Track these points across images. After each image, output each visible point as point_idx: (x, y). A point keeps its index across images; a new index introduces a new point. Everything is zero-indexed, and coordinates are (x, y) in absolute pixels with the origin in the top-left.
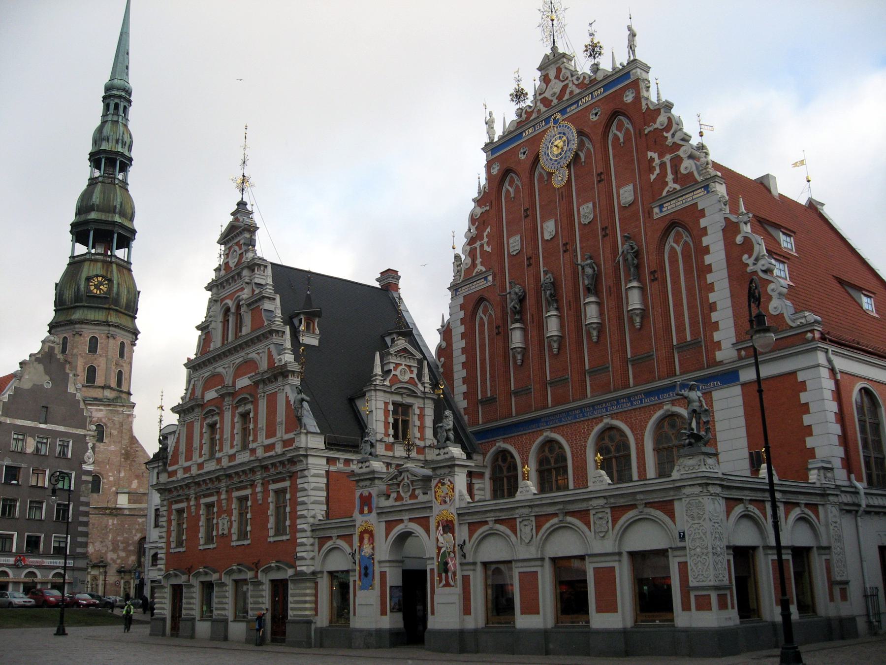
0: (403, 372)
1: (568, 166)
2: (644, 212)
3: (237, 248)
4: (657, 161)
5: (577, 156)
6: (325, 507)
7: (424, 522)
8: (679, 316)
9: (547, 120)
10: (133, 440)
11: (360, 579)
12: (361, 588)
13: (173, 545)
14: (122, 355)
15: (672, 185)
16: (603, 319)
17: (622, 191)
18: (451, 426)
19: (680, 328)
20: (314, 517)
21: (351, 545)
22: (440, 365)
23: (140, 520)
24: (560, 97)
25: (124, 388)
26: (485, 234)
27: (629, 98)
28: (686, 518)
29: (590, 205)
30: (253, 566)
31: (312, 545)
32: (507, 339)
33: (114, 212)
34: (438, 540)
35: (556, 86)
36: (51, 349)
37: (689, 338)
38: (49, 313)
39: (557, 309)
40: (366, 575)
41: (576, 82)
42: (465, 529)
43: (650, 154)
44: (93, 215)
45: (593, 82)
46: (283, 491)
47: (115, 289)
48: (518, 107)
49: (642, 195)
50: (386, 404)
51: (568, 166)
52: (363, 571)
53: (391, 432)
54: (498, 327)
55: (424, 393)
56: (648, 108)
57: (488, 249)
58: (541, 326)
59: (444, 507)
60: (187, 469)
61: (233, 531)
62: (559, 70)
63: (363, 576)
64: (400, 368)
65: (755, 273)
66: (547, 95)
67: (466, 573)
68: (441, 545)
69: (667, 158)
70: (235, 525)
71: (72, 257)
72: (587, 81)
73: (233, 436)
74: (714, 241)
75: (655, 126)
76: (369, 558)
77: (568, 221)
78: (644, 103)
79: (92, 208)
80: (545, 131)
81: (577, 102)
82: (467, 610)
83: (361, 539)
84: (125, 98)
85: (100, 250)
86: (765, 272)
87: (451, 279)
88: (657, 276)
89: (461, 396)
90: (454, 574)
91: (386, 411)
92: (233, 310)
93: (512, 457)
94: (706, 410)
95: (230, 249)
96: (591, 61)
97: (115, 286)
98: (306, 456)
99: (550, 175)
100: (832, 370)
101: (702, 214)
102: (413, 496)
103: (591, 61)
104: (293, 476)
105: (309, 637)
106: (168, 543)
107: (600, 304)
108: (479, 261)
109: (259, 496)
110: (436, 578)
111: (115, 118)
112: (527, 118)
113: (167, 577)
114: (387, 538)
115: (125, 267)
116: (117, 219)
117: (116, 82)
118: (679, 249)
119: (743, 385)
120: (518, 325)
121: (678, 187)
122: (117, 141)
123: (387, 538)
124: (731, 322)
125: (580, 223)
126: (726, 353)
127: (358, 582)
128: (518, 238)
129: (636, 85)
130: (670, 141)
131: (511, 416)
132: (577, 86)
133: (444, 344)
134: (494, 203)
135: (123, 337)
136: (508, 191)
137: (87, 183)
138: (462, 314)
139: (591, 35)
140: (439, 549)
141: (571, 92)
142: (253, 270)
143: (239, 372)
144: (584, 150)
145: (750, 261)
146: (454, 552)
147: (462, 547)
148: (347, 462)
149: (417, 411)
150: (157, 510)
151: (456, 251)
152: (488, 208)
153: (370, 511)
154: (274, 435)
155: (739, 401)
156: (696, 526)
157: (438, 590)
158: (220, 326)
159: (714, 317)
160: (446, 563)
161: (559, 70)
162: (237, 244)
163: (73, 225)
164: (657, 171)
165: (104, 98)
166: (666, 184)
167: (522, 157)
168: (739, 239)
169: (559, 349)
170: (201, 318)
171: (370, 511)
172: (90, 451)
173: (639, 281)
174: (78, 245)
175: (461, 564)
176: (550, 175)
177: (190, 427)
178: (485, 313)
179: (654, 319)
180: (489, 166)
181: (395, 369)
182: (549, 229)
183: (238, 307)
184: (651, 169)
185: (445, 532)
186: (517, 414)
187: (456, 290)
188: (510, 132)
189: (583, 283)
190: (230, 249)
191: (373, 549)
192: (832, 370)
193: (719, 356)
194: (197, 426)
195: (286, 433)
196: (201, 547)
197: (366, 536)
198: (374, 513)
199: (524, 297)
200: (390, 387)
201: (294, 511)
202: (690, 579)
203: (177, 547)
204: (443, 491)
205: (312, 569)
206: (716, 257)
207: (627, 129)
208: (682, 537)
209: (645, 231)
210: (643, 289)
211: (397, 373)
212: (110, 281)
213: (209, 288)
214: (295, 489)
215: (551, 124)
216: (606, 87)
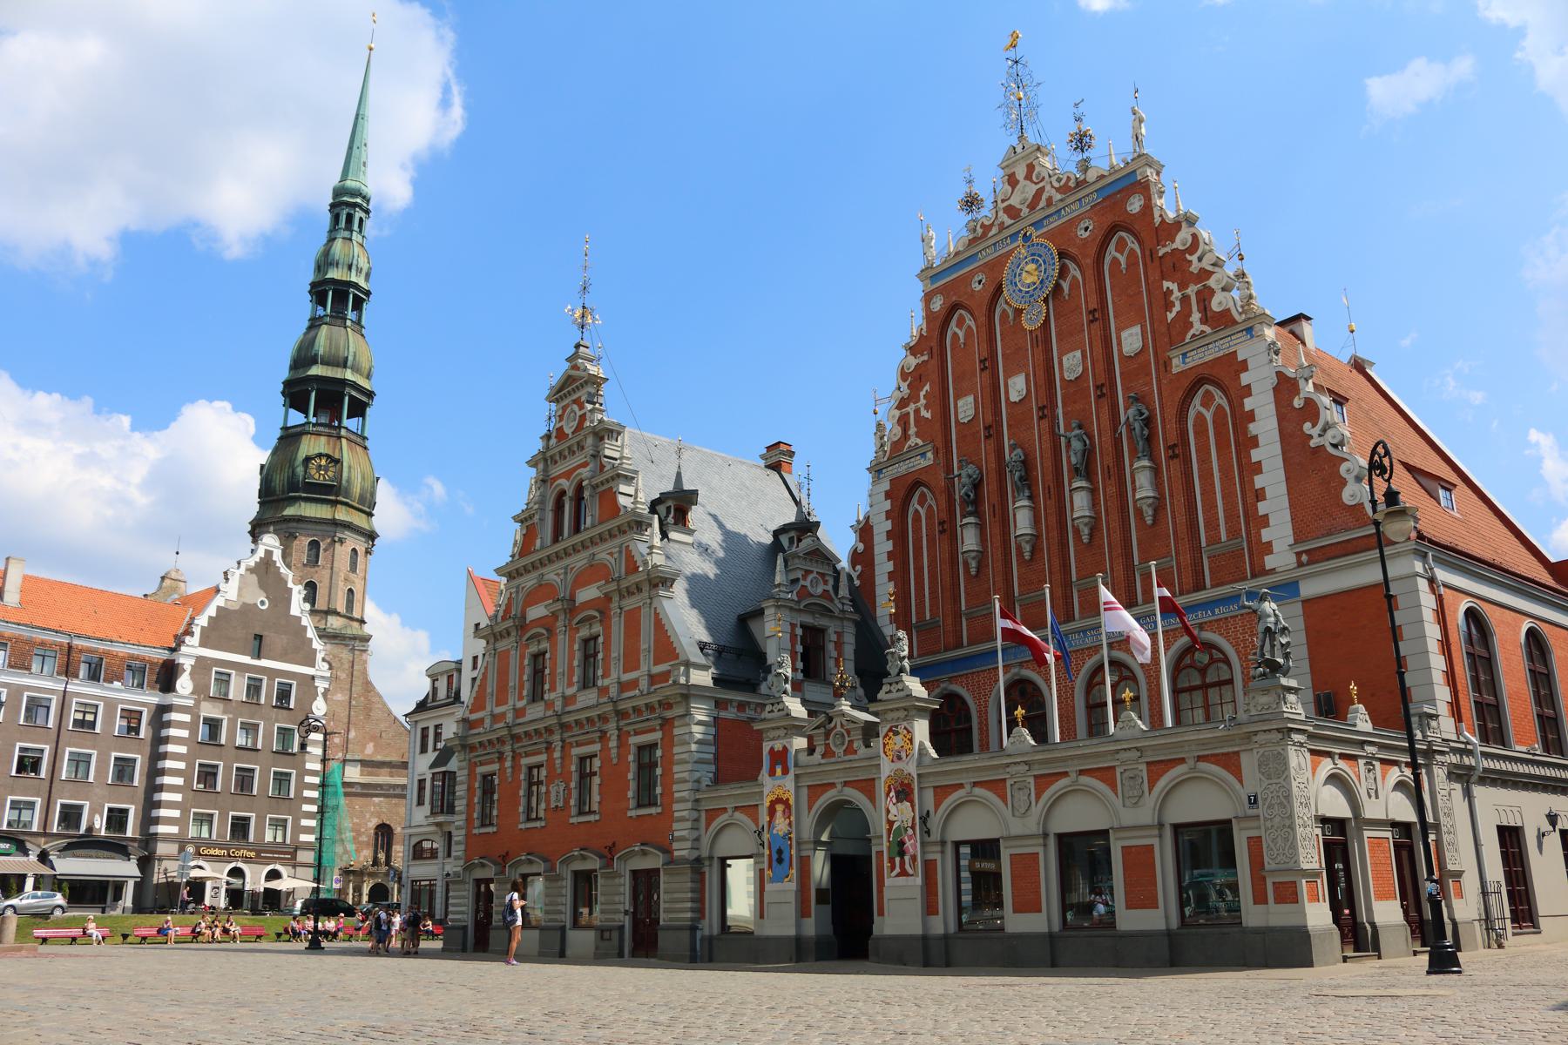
0: (814, 583)
1: (1046, 300)
2: (1157, 363)
3: (575, 407)
4: (1177, 294)
5: (1057, 288)
6: (713, 768)
8: (1210, 506)
9: (1014, 236)
10: (368, 686)
11: (770, 866)
12: (772, 881)
13: (477, 823)
14: (353, 567)
15: (1198, 327)
16: (1098, 513)
17: (1124, 334)
18: (906, 653)
19: (1212, 524)
20: (698, 781)
21: (756, 820)
22: (855, 575)
23: (376, 800)
24: (1032, 206)
25: (356, 615)
26: (922, 393)
27: (1135, 205)
28: (1259, 775)
29: (1078, 354)
30: (606, 852)
31: (697, 820)
32: (953, 539)
33: (345, 366)
34: (888, 811)
35: (1028, 189)
36: (269, 553)
37: (1224, 538)
38: (253, 508)
39: (1030, 498)
40: (780, 861)
41: (1056, 185)
42: (929, 796)
43: (1166, 284)
44: (316, 370)
45: (1080, 184)
46: (653, 746)
47: (345, 475)
48: (969, 217)
49: (1154, 340)
50: (793, 626)
51: (1046, 300)
52: (775, 856)
53: (800, 665)
54: (941, 523)
55: (843, 611)
56: (1163, 221)
57: (927, 414)
58: (1005, 522)
59: (899, 765)
60: (495, 718)
61: (572, 802)
62: (1031, 168)
63: (775, 864)
64: (810, 577)
65: (1321, 448)
66: (1015, 201)
67: (930, 857)
68: (891, 817)
69: (1192, 290)
70: (575, 794)
71: (285, 428)
72: (1072, 184)
73: (571, 668)
74: (1262, 404)
75: (1174, 246)
77: (1046, 375)
78: (1157, 214)
79: (314, 361)
80: (1012, 251)
82: (930, 908)
83: (772, 812)
84: (360, 206)
85: (323, 420)
86: (1335, 446)
87: (872, 456)
88: (1178, 451)
89: (887, 619)
90: (914, 858)
91: (793, 636)
92: (570, 493)
93: (964, 702)
94: (1285, 628)
96: (1079, 157)
97: (345, 470)
99: (1018, 312)
100: (1432, 581)
101: (1244, 366)
102: (850, 750)
103: (1079, 157)
104: (667, 724)
105: (693, 949)
106: (469, 820)
107: (1093, 492)
108: (912, 430)
109: (614, 752)
110: (886, 864)
111: (347, 234)
112: (984, 234)
113: (468, 868)
114: (810, 808)
115: (360, 440)
116: (349, 375)
117: (349, 183)
118: (1209, 416)
119: (1305, 602)
120: (971, 519)
121: (1208, 329)
122: (350, 267)
123: (810, 808)
124: (1286, 516)
125: (1062, 378)
126: (1281, 558)
127: (768, 873)
128: (970, 399)
129: (1143, 188)
130: (1194, 268)
131: (959, 645)
132: (1058, 190)
133: (861, 547)
135: (353, 542)
136: (955, 334)
137: (307, 324)
138: (887, 505)
139: (1078, 120)
140: (891, 823)
141: (1049, 202)
142: (602, 439)
143: (581, 580)
145: (1315, 432)
146: (913, 827)
147: (924, 819)
148: (742, 706)
149: (834, 637)
150: (421, 782)
151: (879, 417)
152: (925, 358)
153: (785, 772)
154: (637, 668)
156: (1272, 788)
157: (887, 882)
158: (549, 517)
159: (1262, 508)
160: (902, 843)
161: (1031, 168)
162: (575, 402)
163: (287, 384)
164: (1177, 308)
165: (333, 206)
167: (977, 287)
169: (1033, 552)
170: (519, 506)
171: (785, 772)
172: (320, 699)
173: (1151, 459)
174: (292, 411)
175: (923, 844)
176: (1018, 312)
177: (503, 658)
178: (921, 503)
179: (1173, 512)
180: (928, 298)
181: (804, 577)
182: (1017, 387)
183: (579, 489)
184: (1169, 306)
185: (899, 800)
186: (970, 644)
187: (879, 471)
188: (957, 254)
189: (1069, 458)
190: (564, 409)
192: (1432, 581)
193: (1270, 562)
194: (514, 656)
195: (656, 664)
196: (522, 826)
198: (791, 776)
199: (981, 480)
200: (798, 602)
201: (668, 772)
202: (1266, 859)
203: (483, 825)
204: (898, 742)
205: (695, 854)
206: (1266, 426)
208: (1253, 801)
209: (1159, 389)
210: (1156, 471)
211: (807, 583)
212: (337, 462)
213: (533, 463)
214: (669, 741)
215: (1020, 241)
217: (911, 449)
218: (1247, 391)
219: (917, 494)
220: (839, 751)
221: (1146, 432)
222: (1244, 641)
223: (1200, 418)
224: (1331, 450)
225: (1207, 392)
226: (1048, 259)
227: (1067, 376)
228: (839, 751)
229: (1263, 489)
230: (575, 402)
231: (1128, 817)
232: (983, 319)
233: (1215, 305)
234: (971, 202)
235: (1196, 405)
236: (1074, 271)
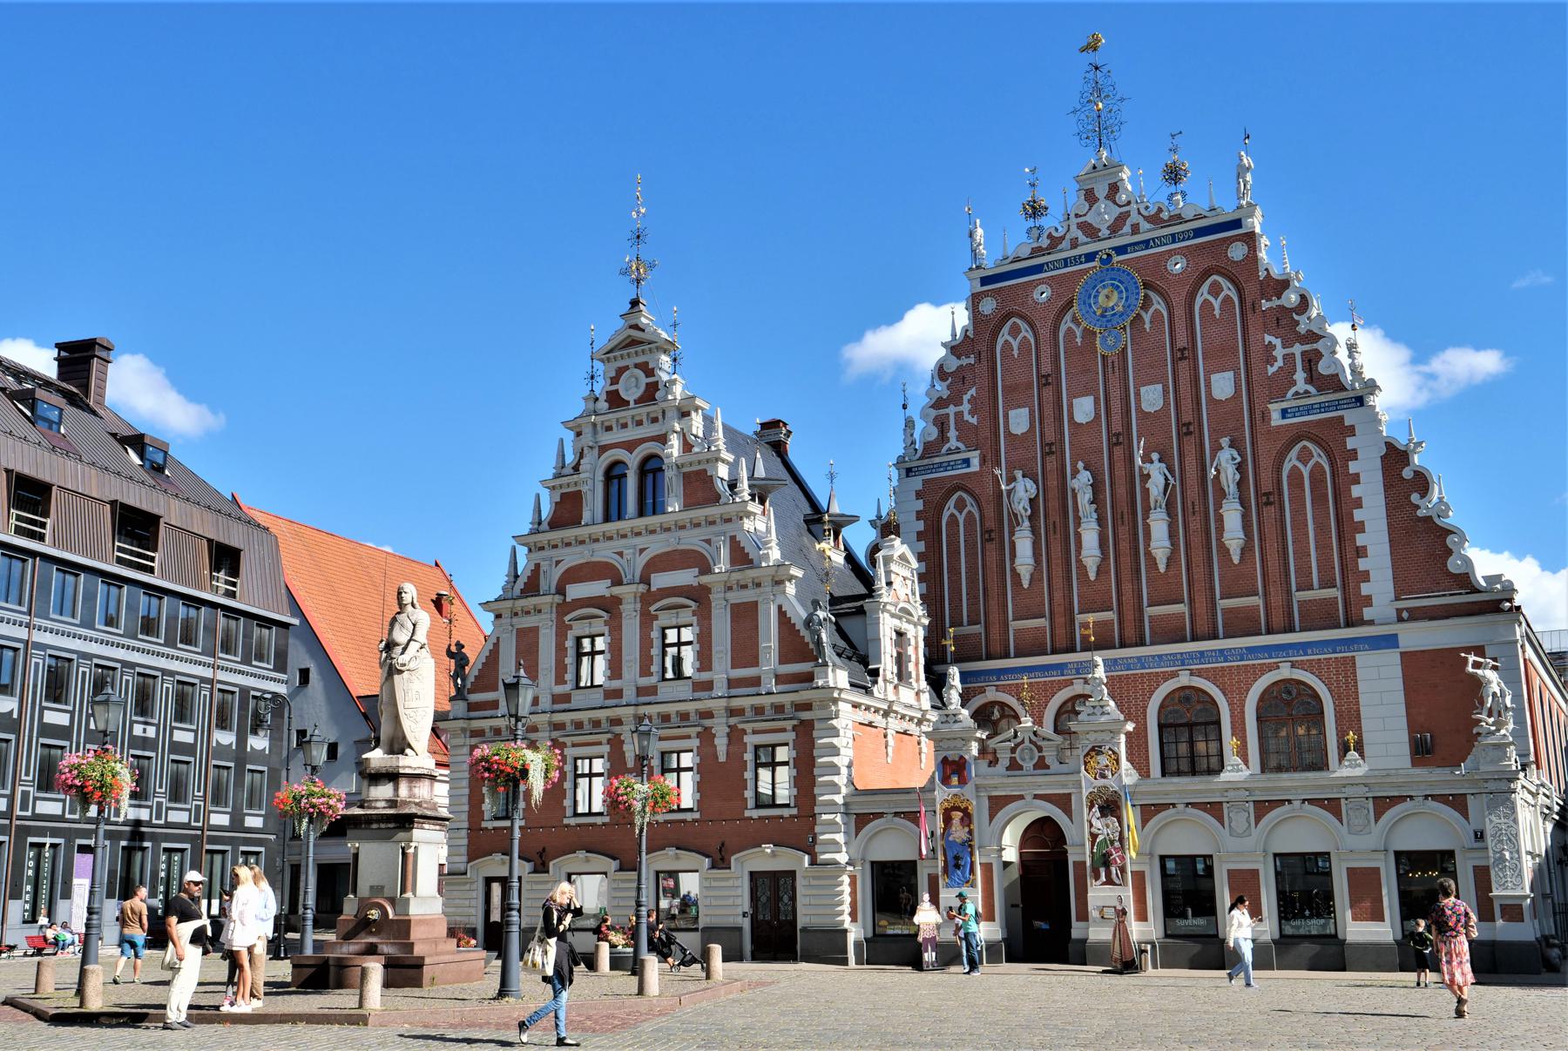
7: (1064, 802)
8: (1302, 554)
12: (948, 886)
19: (1304, 571)
24: (1115, 228)
26: (966, 398)
27: (1237, 252)
29: (1159, 387)
54: (987, 532)
59: (1101, 782)
72: (1165, 215)
76: (963, 844)
80: (1087, 271)
81: (1146, 244)
83: (948, 820)
88: (1270, 498)
90: (1123, 870)
95: (621, 371)
98: (835, 701)
101: (1351, 431)
108: (952, 433)
114: (992, 817)
129: (1250, 239)
130: (1302, 329)
134: (983, 355)
138: (919, 505)
140: (1094, 836)
141: (1135, 229)
144: (1151, 311)
155: (1397, 671)
162: (637, 366)
166: (1294, 383)
168: (1407, 473)
182: (1084, 409)
184: (1271, 360)
185: (1103, 815)
188: (1017, 260)
190: (621, 371)
191: (970, 832)
193: (1368, 613)
197: (957, 815)
207: (1228, 299)
216: (1199, 232)
217: (950, 452)
218: (1353, 455)
219: (955, 497)
220: (1028, 765)
221: (1238, 477)
222: (1338, 681)
223: (1295, 475)
224: (1436, 520)
225: (1305, 447)
226: (1132, 288)
227: (1146, 407)
228: (1028, 765)
229: (1365, 547)
230: (637, 366)
231: (1353, 841)
232: (1045, 332)
233: (1323, 368)
234: (1035, 210)
235: (1291, 461)
236: (1158, 304)
